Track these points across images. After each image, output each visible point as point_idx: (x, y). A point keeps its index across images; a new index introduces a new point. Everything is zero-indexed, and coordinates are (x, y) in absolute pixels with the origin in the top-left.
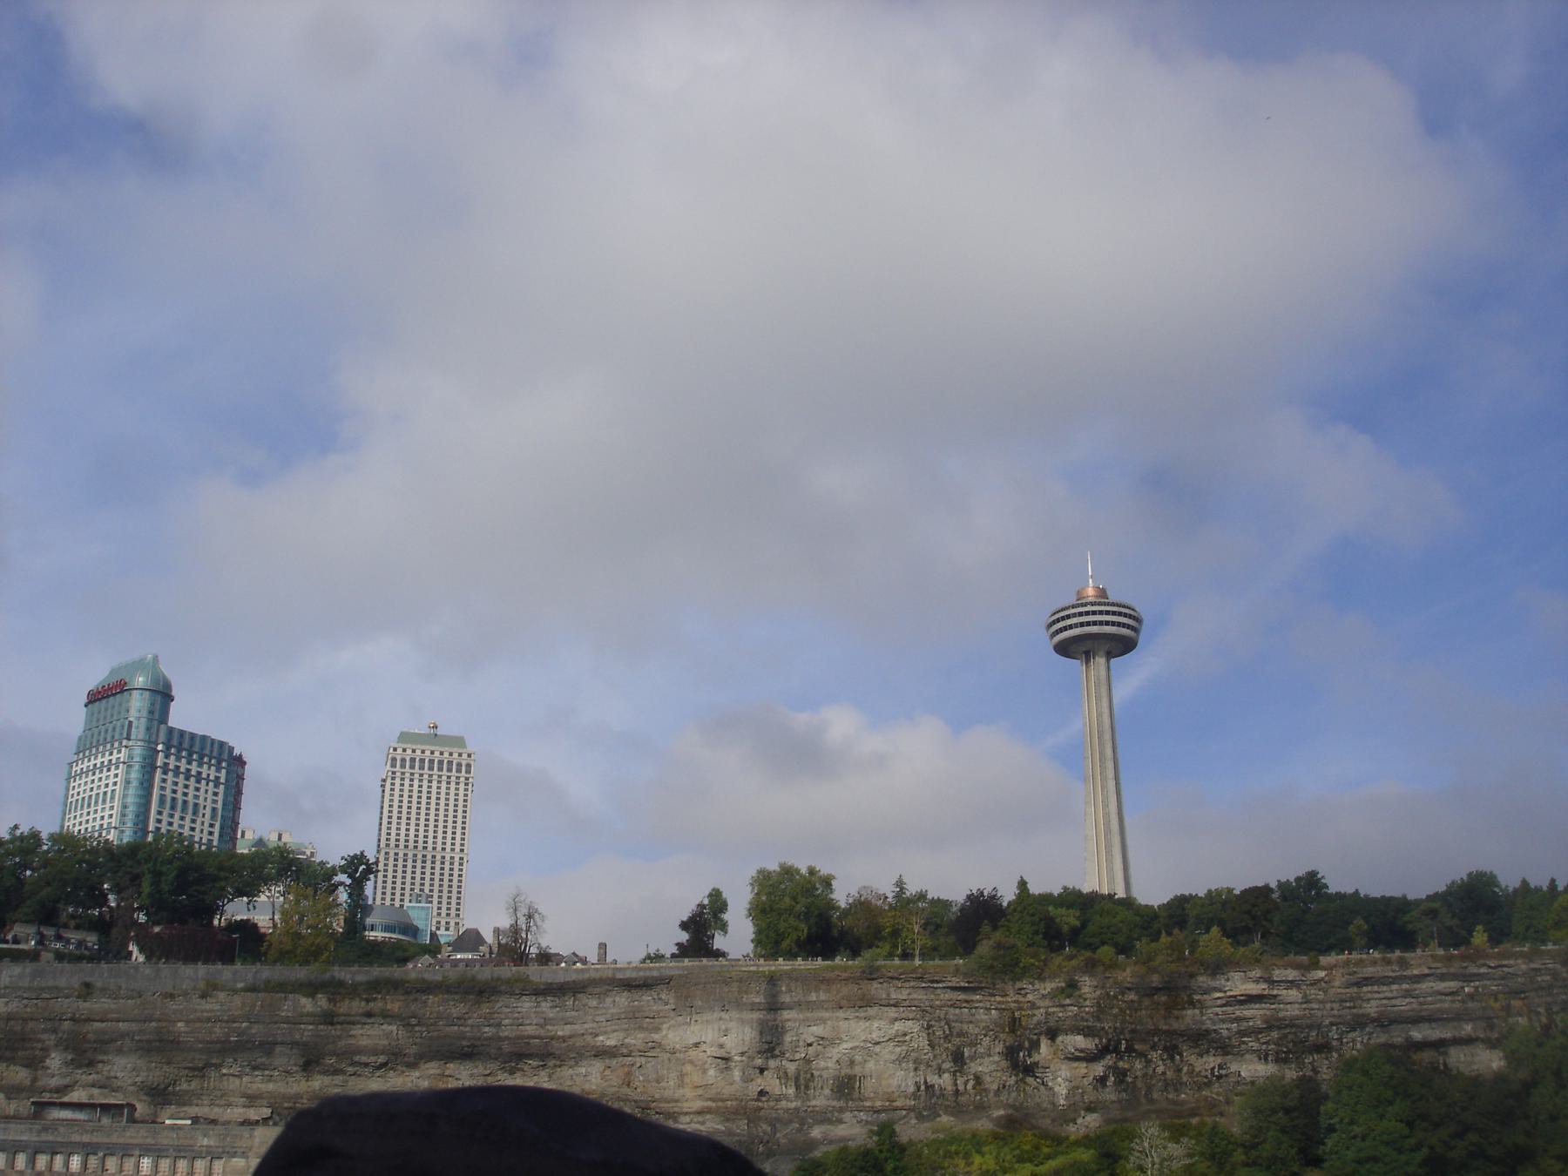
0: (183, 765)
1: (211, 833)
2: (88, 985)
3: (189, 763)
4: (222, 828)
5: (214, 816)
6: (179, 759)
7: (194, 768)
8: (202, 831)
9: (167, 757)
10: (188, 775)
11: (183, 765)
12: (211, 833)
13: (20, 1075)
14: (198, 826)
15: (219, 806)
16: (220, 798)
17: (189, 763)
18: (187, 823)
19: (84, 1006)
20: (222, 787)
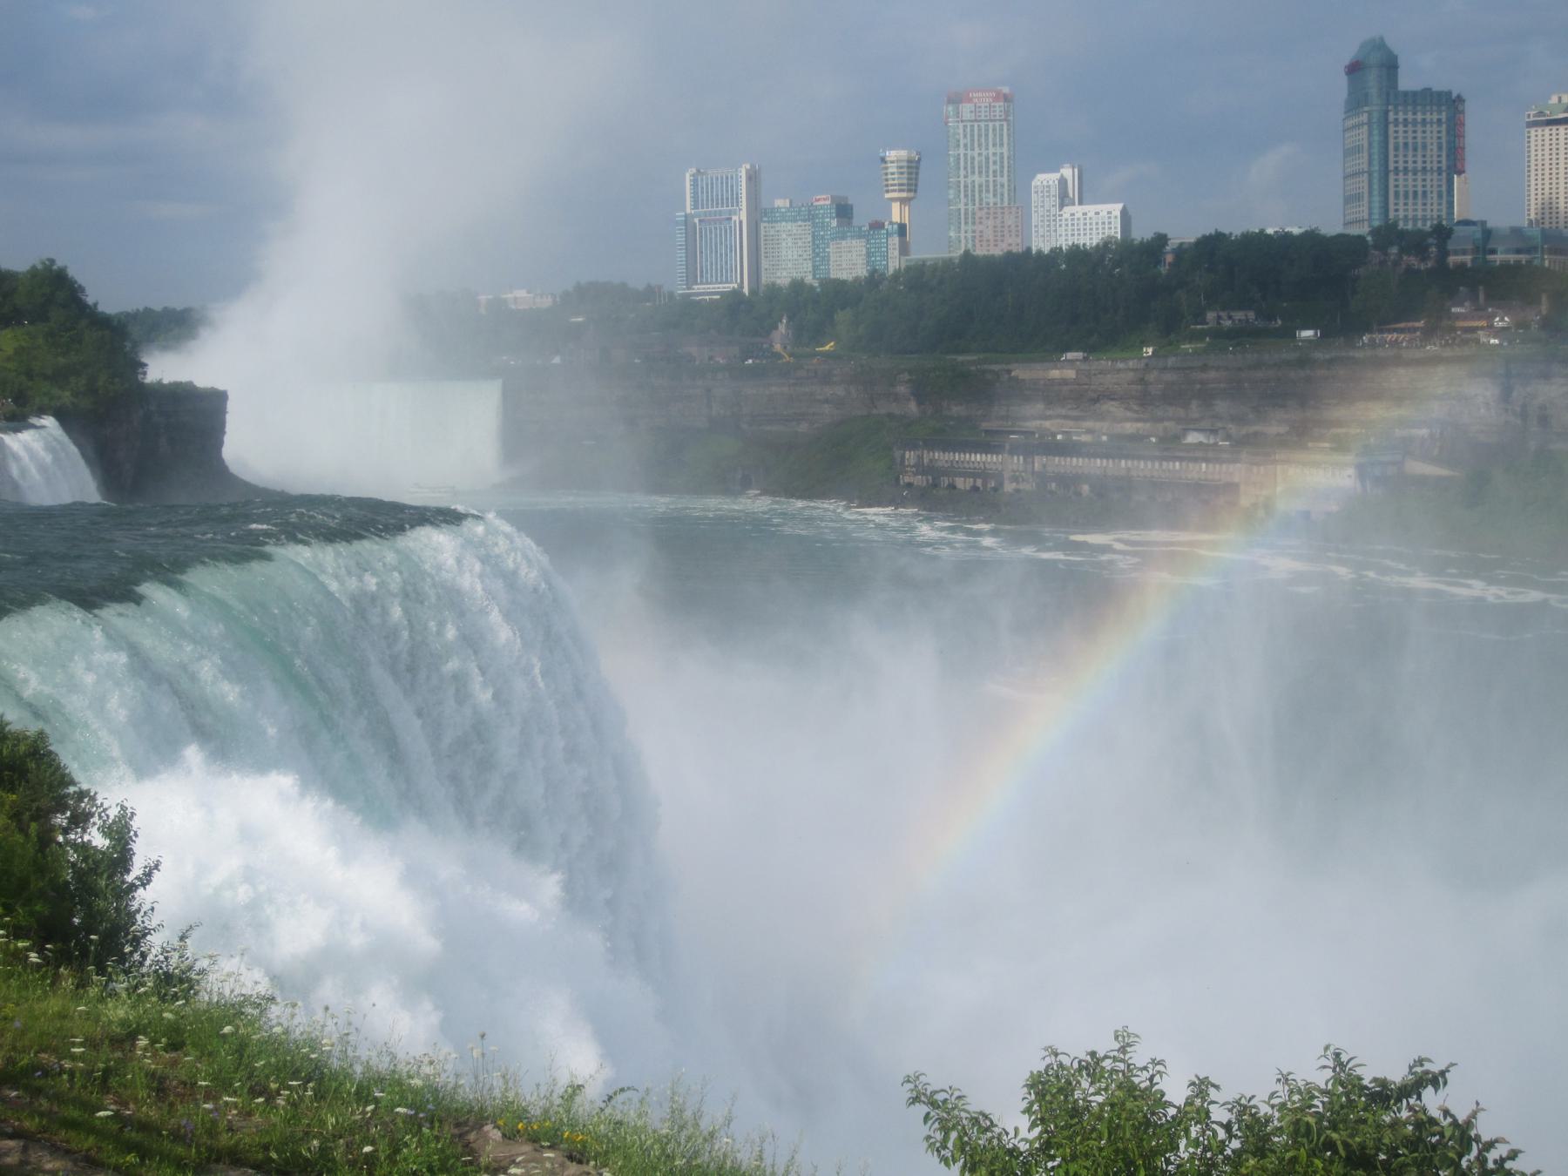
0: (1410, 116)
1: (1439, 162)
2: (1205, 365)
3: (1415, 114)
4: (1448, 156)
5: (1440, 148)
6: (1405, 113)
7: (1419, 117)
8: (1431, 162)
9: (1396, 113)
10: (1415, 123)
11: (1410, 116)
12: (1439, 162)
13: (1181, 412)
14: (1428, 159)
15: (1444, 140)
16: (1444, 134)
17: (1415, 114)
18: (1420, 159)
19: (1204, 376)
20: (1444, 126)
